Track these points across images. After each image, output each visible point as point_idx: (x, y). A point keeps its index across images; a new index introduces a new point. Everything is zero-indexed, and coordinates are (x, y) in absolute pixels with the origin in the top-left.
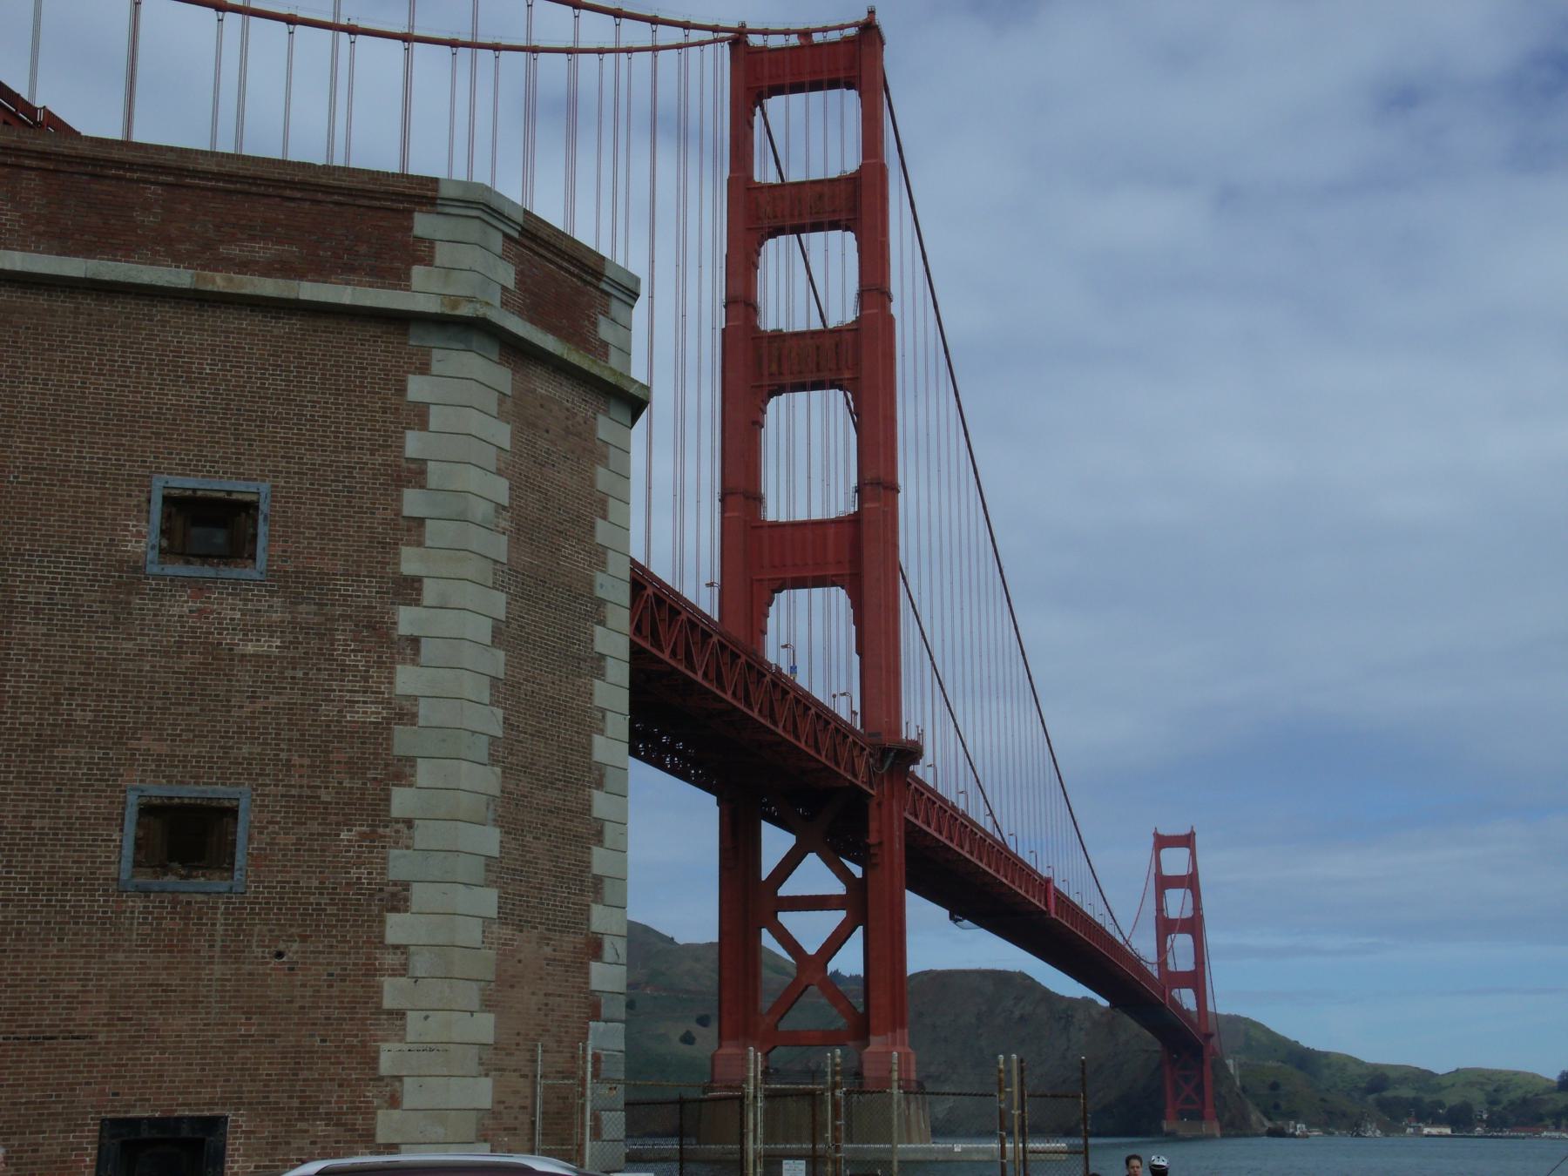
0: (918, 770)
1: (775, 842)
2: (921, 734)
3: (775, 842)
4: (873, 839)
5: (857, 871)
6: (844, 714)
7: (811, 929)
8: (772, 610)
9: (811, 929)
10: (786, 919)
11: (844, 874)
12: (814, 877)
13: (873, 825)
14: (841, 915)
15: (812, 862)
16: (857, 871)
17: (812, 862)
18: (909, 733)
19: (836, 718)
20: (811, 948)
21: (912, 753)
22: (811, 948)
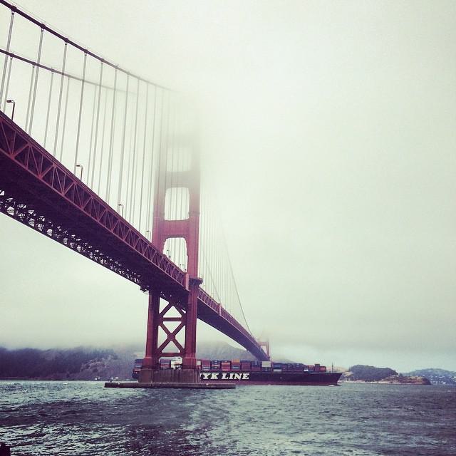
0: (200, 285)
1: (163, 303)
2: (203, 276)
3: (163, 303)
4: (189, 303)
5: (185, 312)
6: (183, 270)
7: (172, 326)
8: (166, 243)
9: (172, 326)
10: (165, 323)
11: (181, 313)
12: (173, 312)
13: (189, 300)
14: (180, 322)
15: (173, 308)
16: (185, 312)
17: (173, 308)
18: (199, 276)
19: (181, 271)
20: (171, 331)
21: (200, 281)
22: (171, 331)
